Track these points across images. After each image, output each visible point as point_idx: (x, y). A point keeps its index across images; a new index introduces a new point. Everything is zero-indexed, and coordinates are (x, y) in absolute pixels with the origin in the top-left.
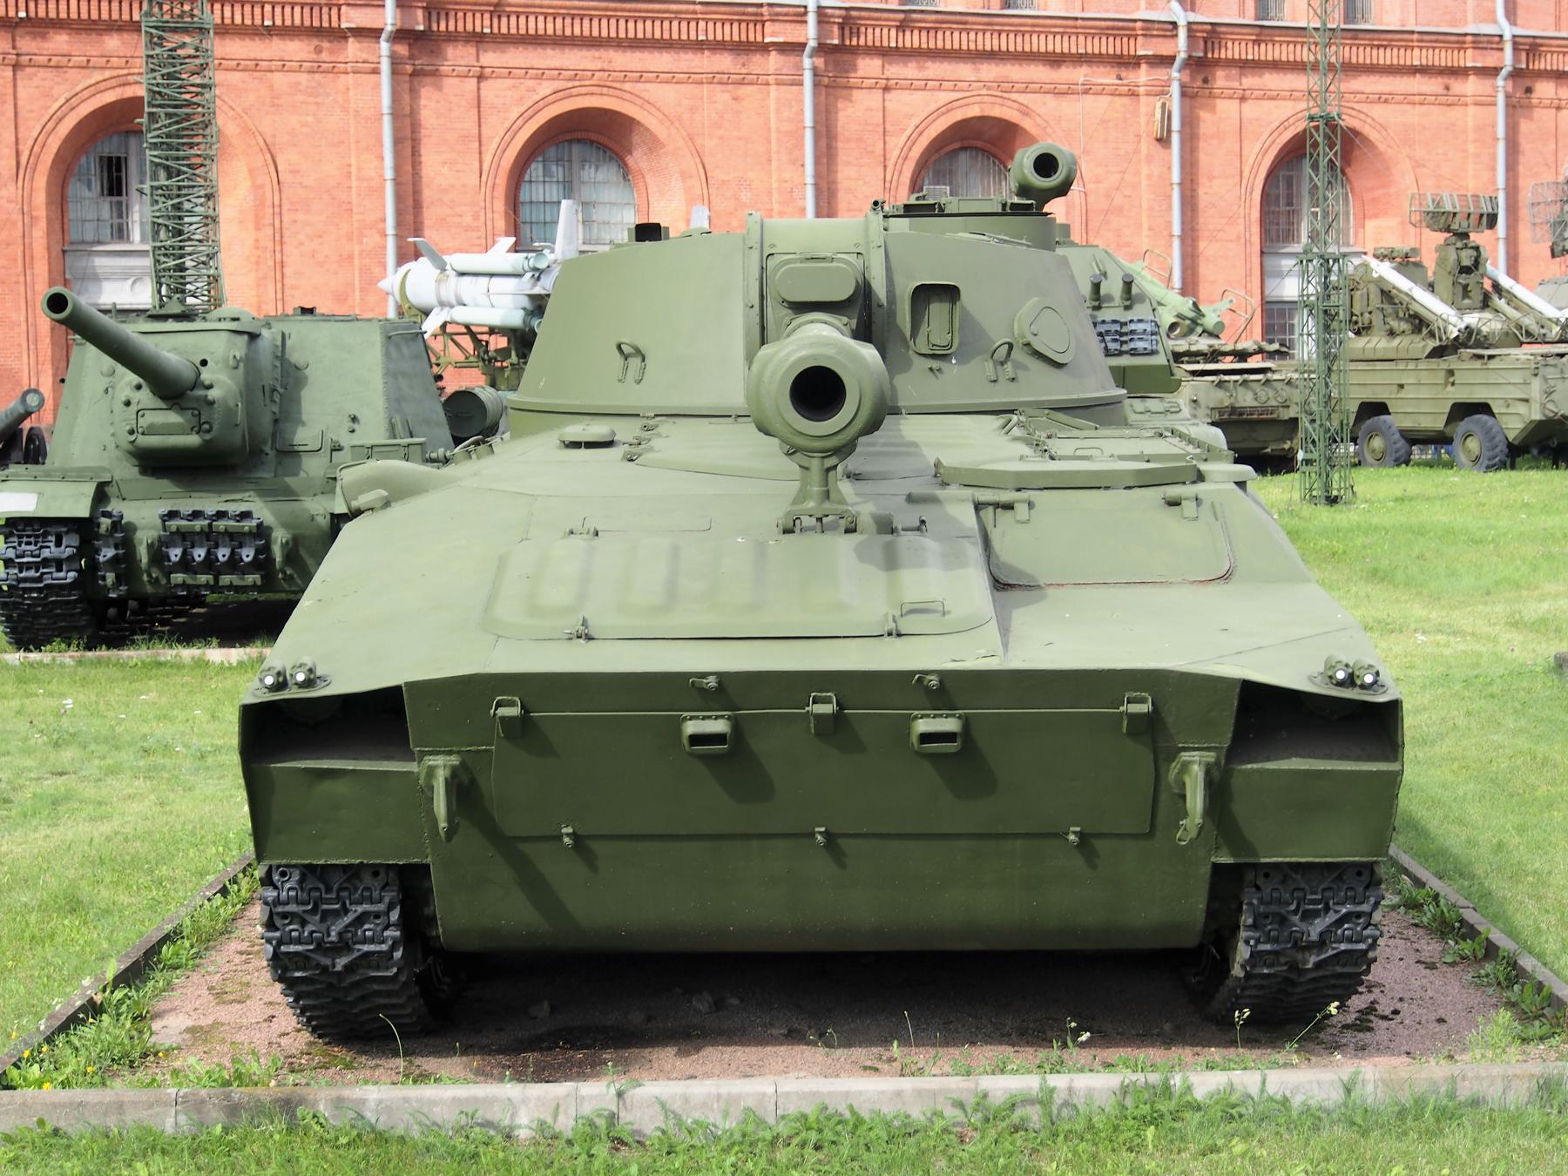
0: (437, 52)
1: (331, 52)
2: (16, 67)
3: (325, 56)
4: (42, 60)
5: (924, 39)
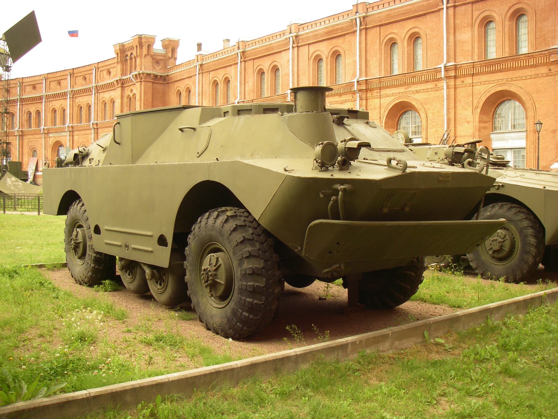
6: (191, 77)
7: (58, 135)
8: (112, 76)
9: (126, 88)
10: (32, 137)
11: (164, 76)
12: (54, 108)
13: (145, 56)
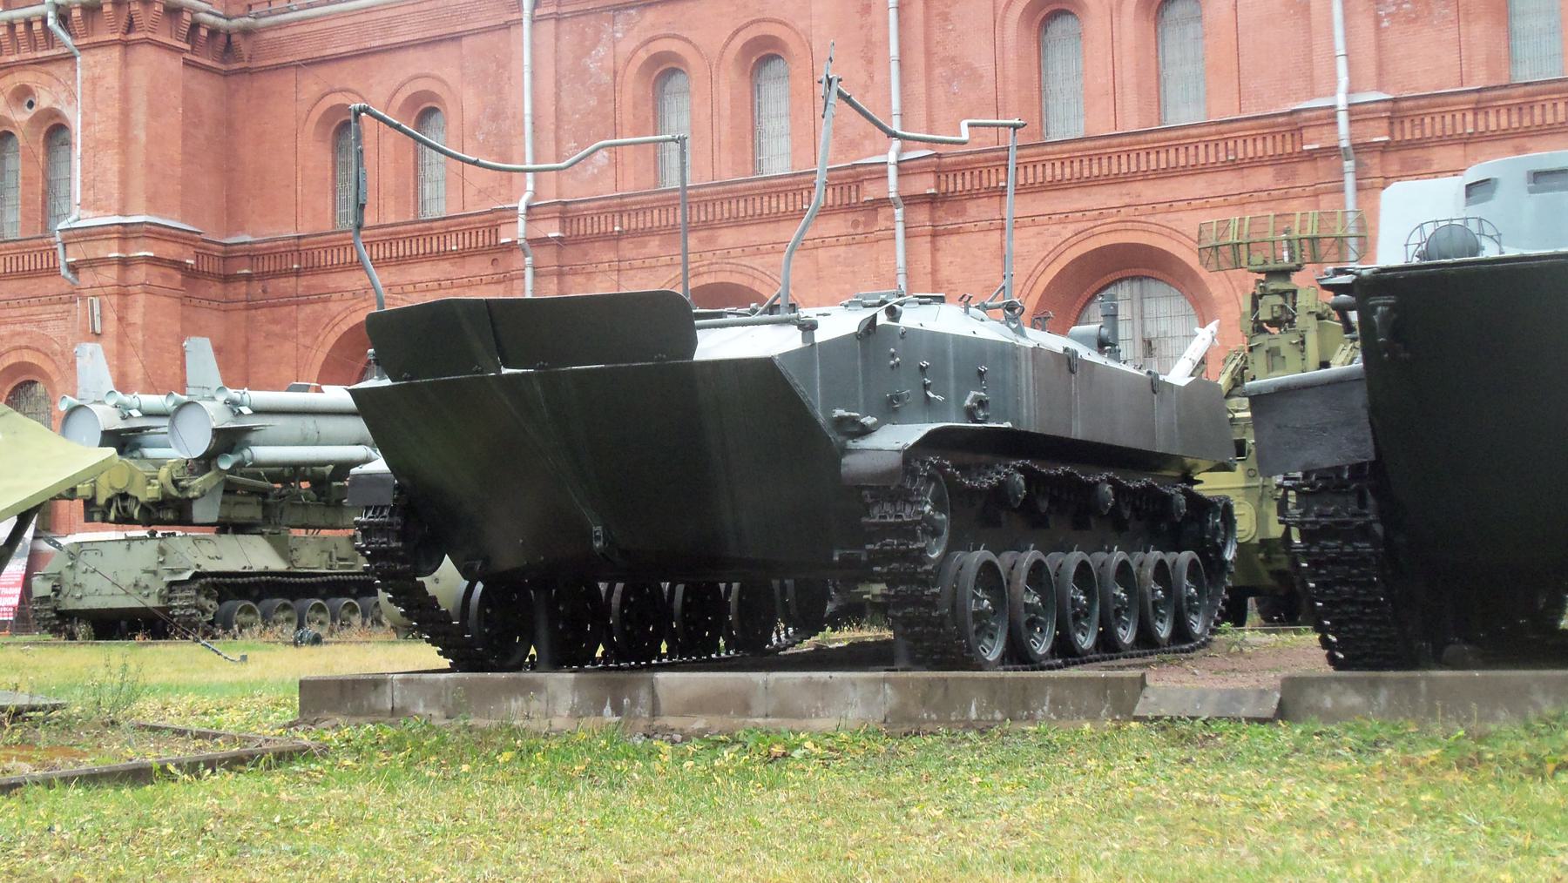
0: (963, 212)
1: (866, 224)
3: (860, 230)
4: (638, 263)
5: (1515, 118)
6: (456, 38)
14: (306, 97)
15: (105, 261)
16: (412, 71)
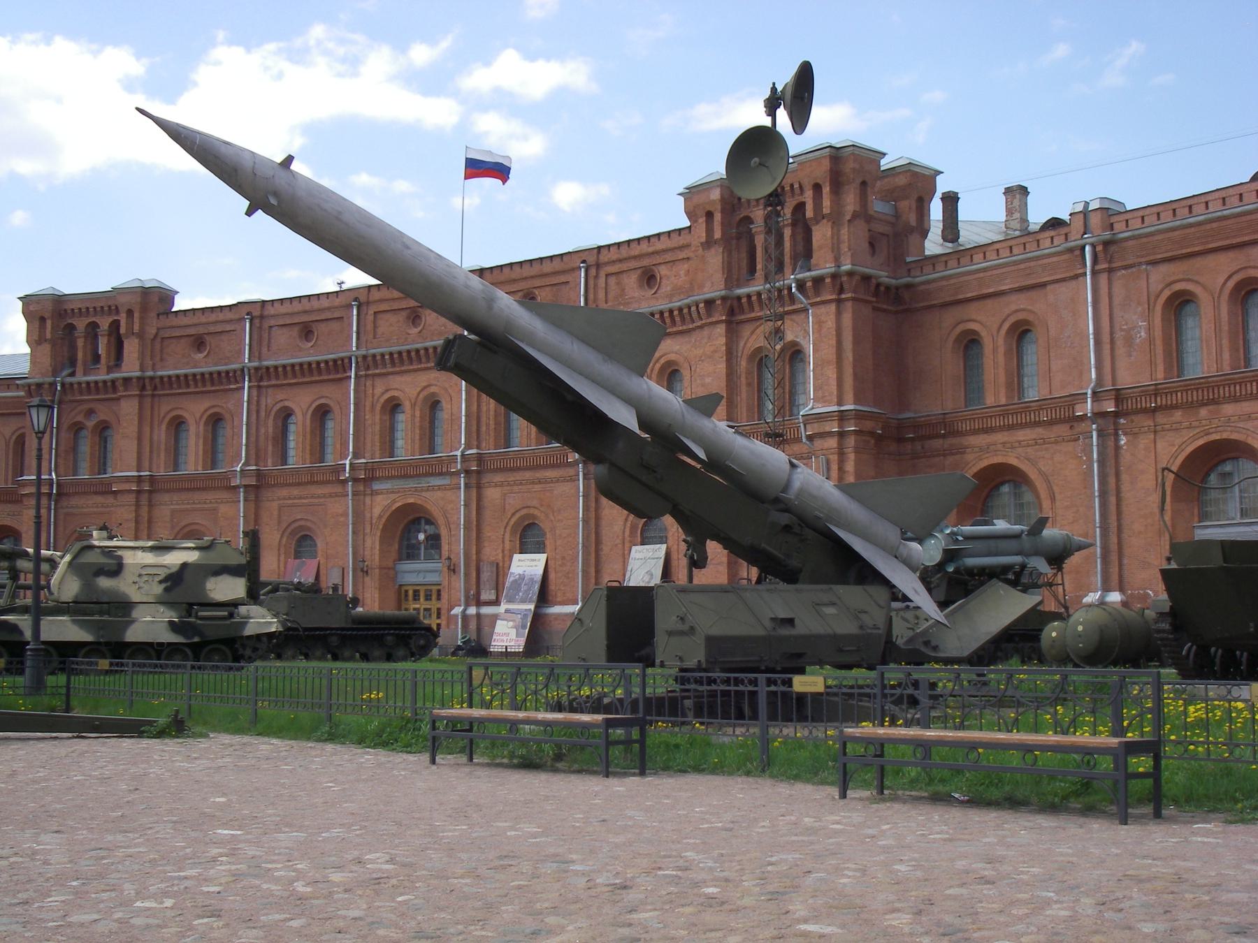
2: (1155, 432)
6: (1043, 285)
7: (411, 484)
8: (666, 288)
9: (746, 330)
10: (295, 491)
11: (897, 288)
12: (393, 398)
13: (855, 216)
14: (946, 326)
15: (830, 434)
16: (1014, 307)
